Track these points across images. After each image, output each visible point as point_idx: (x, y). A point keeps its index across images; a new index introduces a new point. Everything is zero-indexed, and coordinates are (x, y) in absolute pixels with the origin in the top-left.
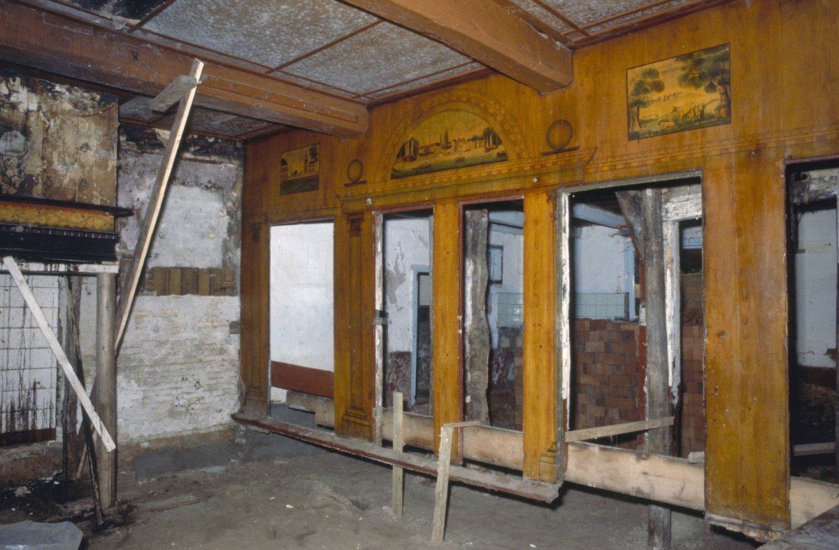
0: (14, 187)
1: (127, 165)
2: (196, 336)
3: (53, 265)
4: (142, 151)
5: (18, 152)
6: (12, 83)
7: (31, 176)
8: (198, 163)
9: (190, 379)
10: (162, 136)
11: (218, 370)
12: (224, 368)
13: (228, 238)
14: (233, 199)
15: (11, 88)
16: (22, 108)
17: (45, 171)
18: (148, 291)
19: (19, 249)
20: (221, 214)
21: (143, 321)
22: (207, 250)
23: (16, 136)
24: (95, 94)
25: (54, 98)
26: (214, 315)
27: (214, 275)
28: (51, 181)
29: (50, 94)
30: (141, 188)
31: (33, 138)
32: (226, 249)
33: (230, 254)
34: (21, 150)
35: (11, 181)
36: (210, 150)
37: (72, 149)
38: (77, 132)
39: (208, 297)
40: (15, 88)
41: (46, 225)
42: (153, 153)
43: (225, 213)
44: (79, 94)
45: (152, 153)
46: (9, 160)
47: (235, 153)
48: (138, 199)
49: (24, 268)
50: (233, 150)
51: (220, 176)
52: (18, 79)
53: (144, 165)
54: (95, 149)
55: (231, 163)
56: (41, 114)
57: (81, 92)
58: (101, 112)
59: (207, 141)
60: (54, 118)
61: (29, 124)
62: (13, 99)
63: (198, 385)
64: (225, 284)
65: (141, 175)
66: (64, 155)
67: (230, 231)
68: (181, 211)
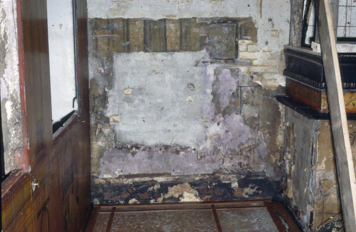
1: (232, 159)
4: (214, 176)
8: (150, 173)
10: (192, 195)
13: (106, 90)
18: (206, 24)
20: (116, 118)
22: (133, 74)
27: (123, 44)
30: (216, 137)
32: (109, 77)
33: (103, 71)
36: (134, 189)
42: (202, 175)
43: (111, 120)
45: (204, 175)
47: (101, 191)
48: (218, 124)
50: (104, 194)
51: (121, 162)
53: (213, 161)
55: (105, 179)
59: (138, 199)
65: (216, 150)
67: (104, 99)
68: (169, 115)
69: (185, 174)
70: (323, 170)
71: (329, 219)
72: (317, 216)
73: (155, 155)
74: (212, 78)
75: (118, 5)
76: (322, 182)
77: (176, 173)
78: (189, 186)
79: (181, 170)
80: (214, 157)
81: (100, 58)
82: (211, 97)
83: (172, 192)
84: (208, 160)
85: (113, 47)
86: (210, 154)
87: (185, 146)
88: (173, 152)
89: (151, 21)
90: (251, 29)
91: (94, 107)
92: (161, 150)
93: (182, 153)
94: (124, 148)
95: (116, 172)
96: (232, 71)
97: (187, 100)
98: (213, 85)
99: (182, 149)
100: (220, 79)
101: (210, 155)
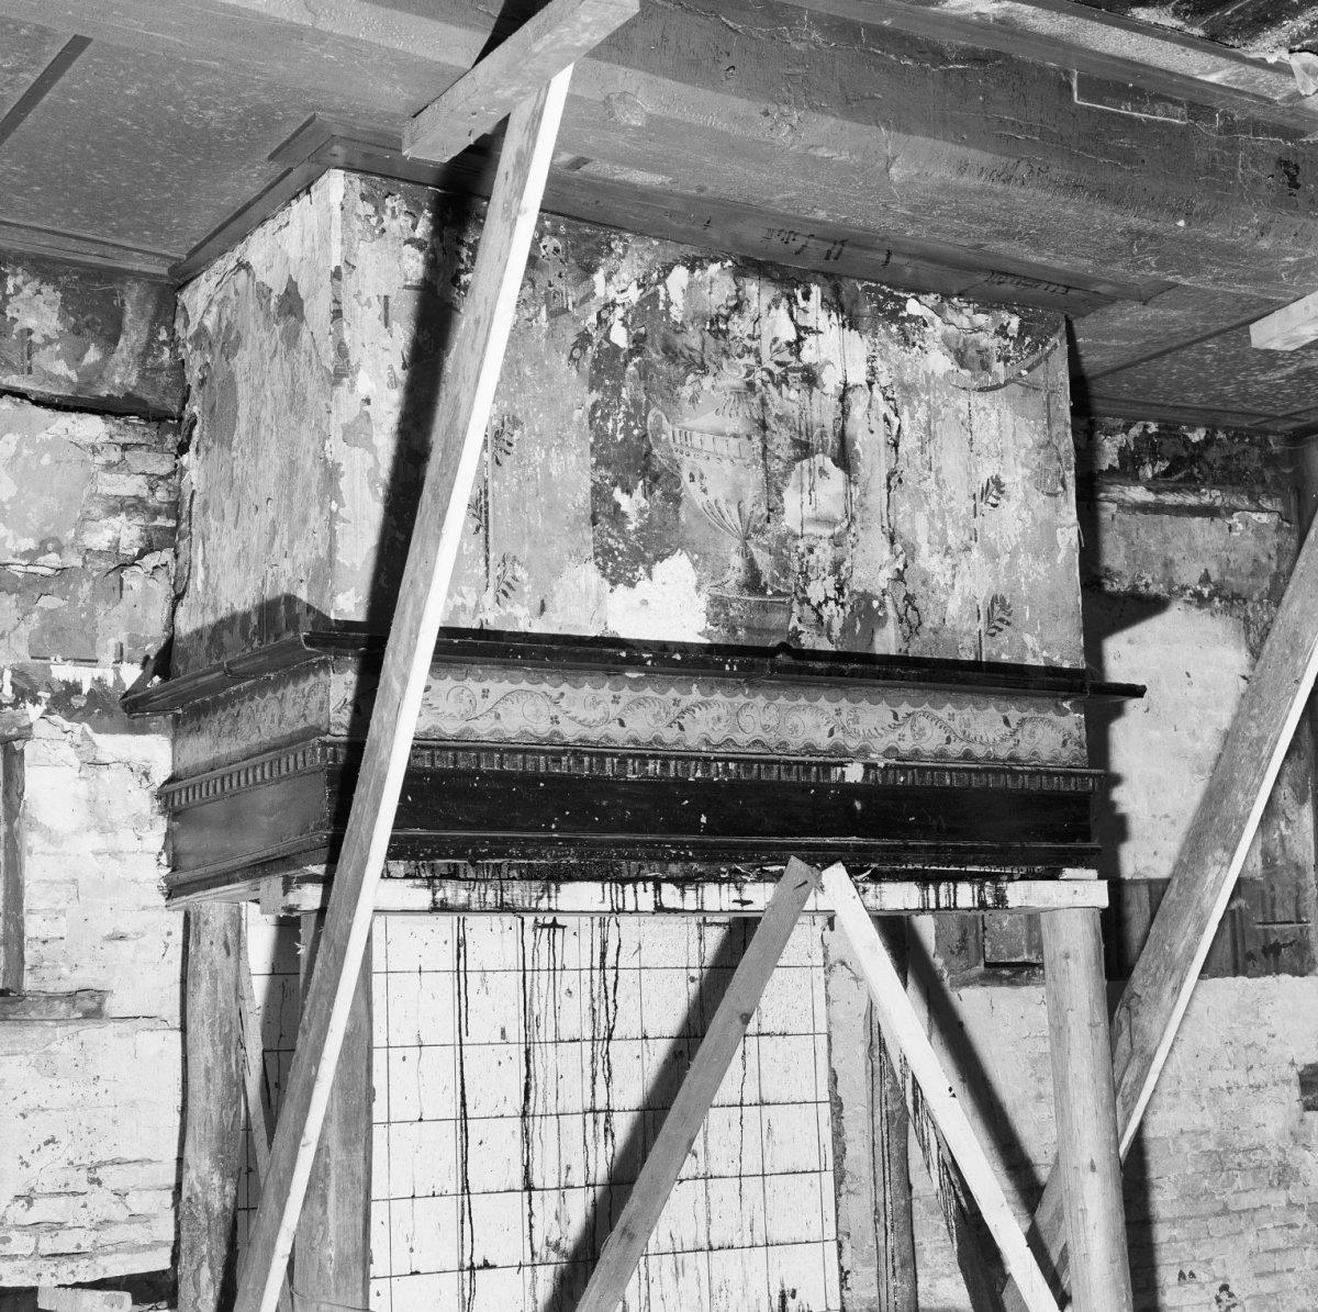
0: (829, 637)
2: (1207, 1119)
3: (943, 888)
5: (831, 523)
6: (802, 303)
7: (866, 597)
9: (1202, 1277)
11: (1277, 1240)
12: (1296, 1233)
15: (801, 322)
16: (831, 380)
17: (900, 577)
19: (854, 840)
23: (822, 472)
24: (1005, 316)
25: (906, 341)
26: (1252, 1045)
28: (915, 609)
29: (894, 329)
31: (863, 470)
33: (1283, 824)
34: (839, 517)
35: (820, 617)
37: (963, 505)
38: (971, 442)
39: (1230, 980)
40: (809, 321)
41: (916, 754)
44: (966, 319)
46: (811, 551)
47: (1268, 475)
49: (871, 901)
51: (1233, 556)
52: (816, 290)
54: (1021, 495)
55: (1264, 511)
56: (878, 395)
57: (969, 312)
58: (1024, 372)
60: (910, 404)
61: (849, 432)
62: (808, 355)
63: (1224, 1296)
66: (944, 524)
70: (1061, 526)
71: (1029, 370)
76: (1060, 489)
81: (1289, 862)
85: (1263, 892)
90: (952, 952)
94: (1226, 598)
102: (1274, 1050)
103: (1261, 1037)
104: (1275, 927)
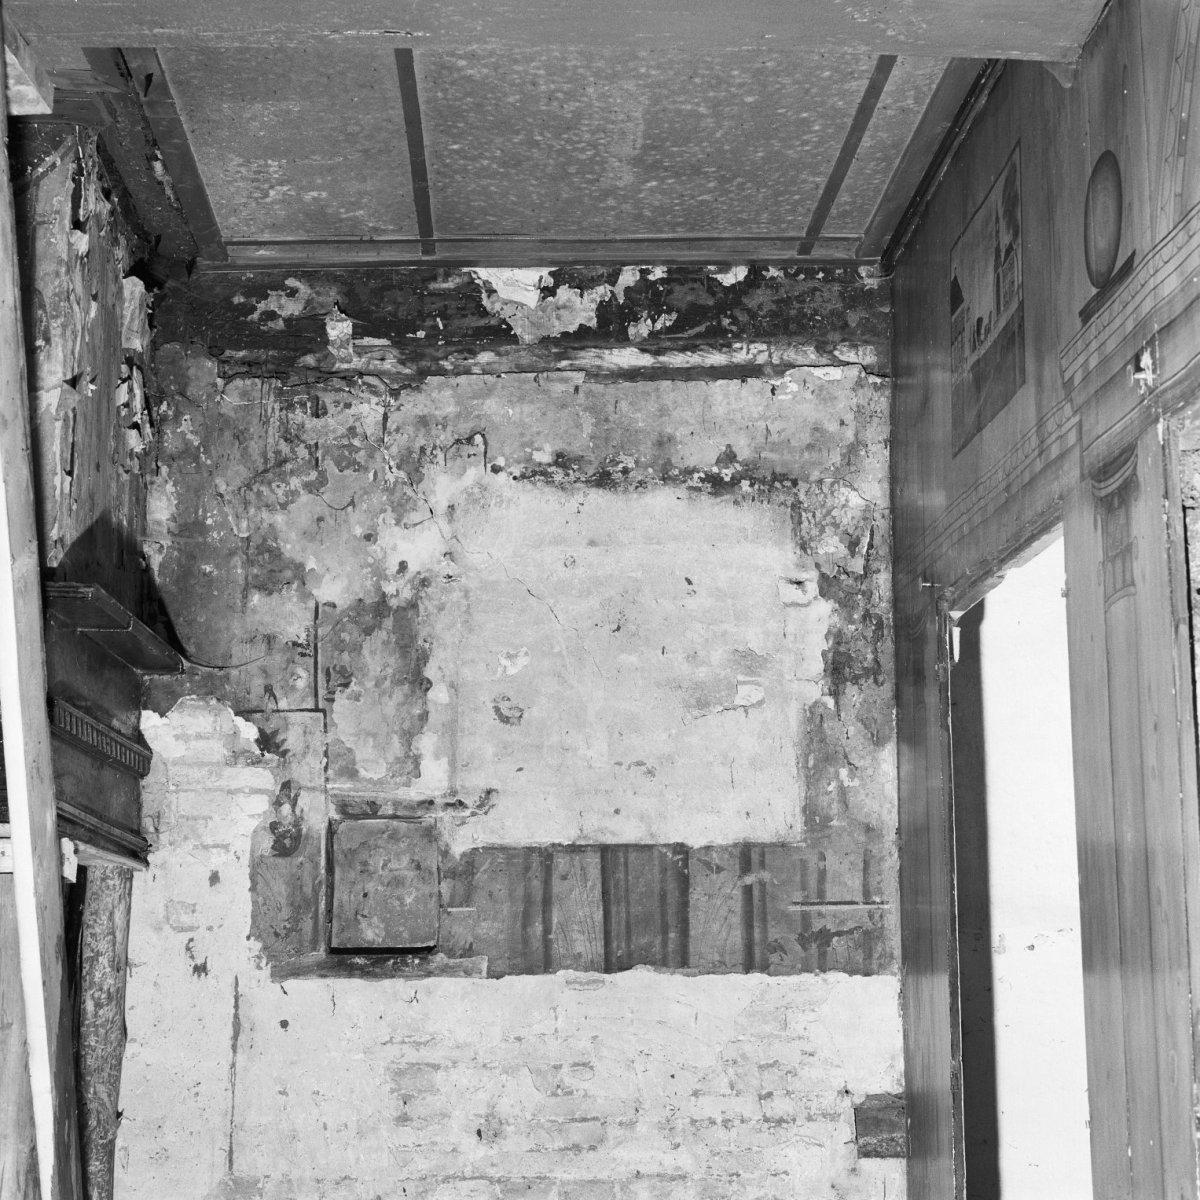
1: (352, 431)
2: (684, 1160)
4: (421, 368)
10: (503, 293)
13: (830, 702)
14: (846, 519)
18: (451, 954)
20: (794, 594)
21: (433, 1090)
27: (766, 875)
30: (414, 517)
32: (820, 752)
33: (844, 772)
36: (726, 322)
42: (468, 372)
43: (812, 588)
50: (839, 306)
53: (423, 421)
55: (838, 363)
59: (713, 286)
64: (827, 917)
65: (414, 465)
67: (839, 669)
68: (594, 602)
69: (532, 375)
72: (57, 212)
73: (646, 451)
74: (426, 743)
75: (785, 1025)
77: (565, 381)
78: (517, 331)
79: (545, 392)
80: (421, 442)
81: (853, 821)
82: (430, 672)
83: (580, 308)
84: (444, 427)
85: (804, 863)
86: (438, 452)
87: (534, 484)
88: (579, 459)
89: (661, 963)
90: (277, 935)
91: (878, 636)
92: (625, 471)
93: (544, 457)
94: (763, 481)
95: (794, 387)
96: (351, 773)
97: (522, 661)
98: (424, 717)
99: (544, 473)
100: (396, 739)
101: (435, 448)
102: (811, 1073)
103: (789, 1054)
104: (823, 909)
